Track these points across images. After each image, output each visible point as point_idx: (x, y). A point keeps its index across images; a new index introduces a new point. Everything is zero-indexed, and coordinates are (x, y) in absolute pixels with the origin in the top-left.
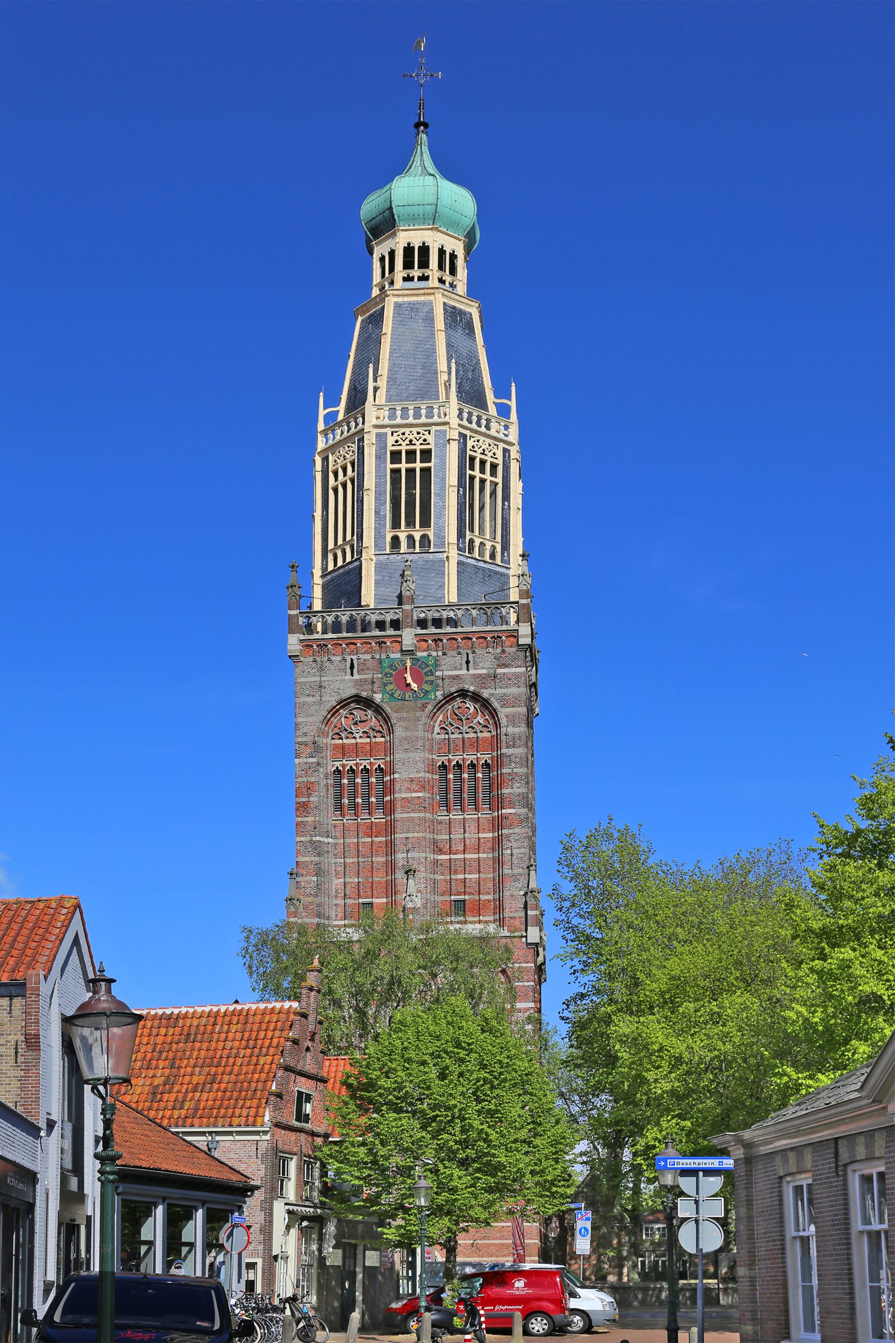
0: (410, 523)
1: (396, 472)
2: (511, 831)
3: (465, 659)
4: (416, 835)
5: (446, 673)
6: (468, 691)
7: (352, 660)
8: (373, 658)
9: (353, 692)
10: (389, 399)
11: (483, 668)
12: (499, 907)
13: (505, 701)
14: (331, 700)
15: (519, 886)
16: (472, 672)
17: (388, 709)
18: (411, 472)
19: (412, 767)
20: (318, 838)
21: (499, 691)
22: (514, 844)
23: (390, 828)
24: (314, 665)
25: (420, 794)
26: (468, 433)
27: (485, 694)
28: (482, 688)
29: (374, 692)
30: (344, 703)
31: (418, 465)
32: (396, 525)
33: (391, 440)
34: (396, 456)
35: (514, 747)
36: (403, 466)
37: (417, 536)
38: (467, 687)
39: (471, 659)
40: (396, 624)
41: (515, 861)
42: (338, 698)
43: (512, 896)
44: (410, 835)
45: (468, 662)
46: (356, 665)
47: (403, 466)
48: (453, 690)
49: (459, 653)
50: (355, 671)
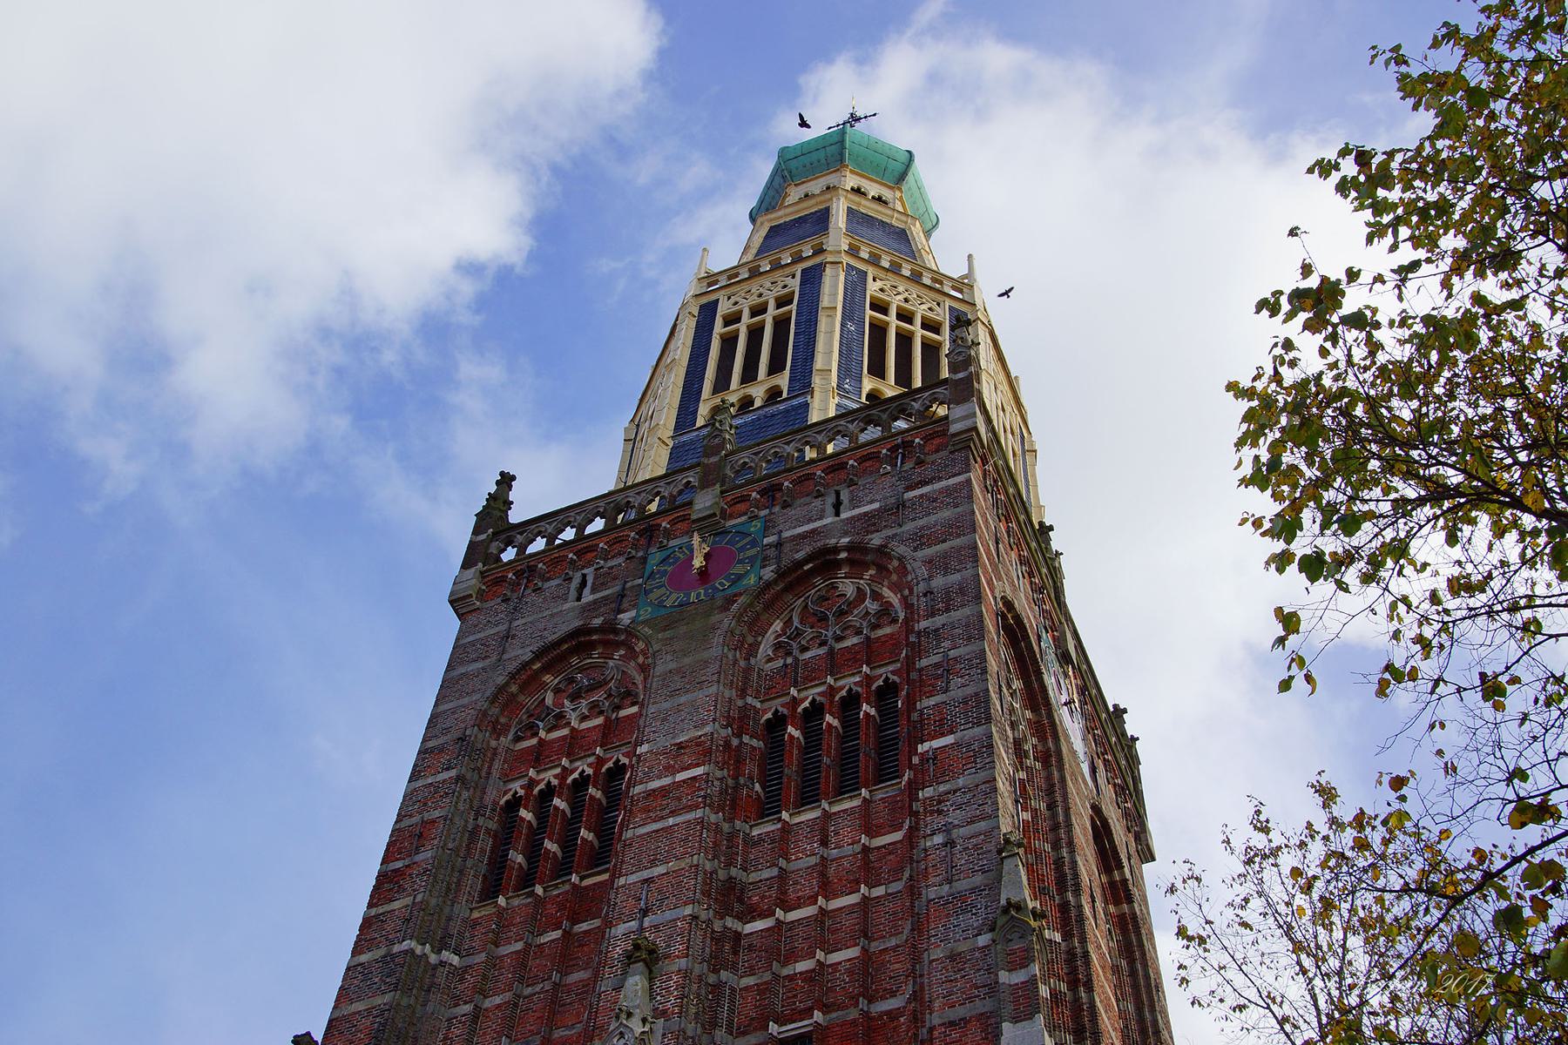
0: (749, 375)
1: (729, 342)
2: (942, 788)
3: (831, 499)
5: (786, 534)
6: (836, 550)
7: (584, 576)
9: (577, 623)
11: (872, 502)
13: (920, 540)
14: (521, 652)
15: (975, 922)
16: (844, 516)
18: (755, 334)
20: (406, 945)
21: (909, 527)
22: (955, 817)
25: (699, 771)
26: (871, 272)
28: (868, 532)
29: (620, 612)
30: (555, 655)
35: (947, 610)
41: (961, 860)
43: (953, 957)
46: (589, 584)
48: (800, 555)
49: (819, 495)
50: (587, 591)
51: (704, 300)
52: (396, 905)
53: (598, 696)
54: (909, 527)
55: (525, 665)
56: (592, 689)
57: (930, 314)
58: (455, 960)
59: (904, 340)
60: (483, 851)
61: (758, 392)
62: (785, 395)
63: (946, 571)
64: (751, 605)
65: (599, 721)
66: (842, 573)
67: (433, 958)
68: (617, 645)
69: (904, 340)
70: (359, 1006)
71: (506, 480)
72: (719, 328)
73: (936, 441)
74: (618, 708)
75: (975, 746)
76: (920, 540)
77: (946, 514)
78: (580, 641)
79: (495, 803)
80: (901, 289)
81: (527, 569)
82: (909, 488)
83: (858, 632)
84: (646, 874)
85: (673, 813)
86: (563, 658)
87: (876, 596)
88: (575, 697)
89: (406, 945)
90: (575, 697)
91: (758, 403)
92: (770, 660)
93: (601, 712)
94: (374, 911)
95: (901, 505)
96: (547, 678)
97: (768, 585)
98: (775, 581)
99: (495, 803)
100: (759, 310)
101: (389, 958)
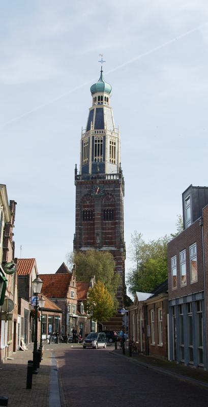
1: (96, 145)
10: (95, 129)
12: (115, 243)
14: (83, 195)
18: (99, 145)
19: (98, 211)
21: (116, 194)
23: (94, 224)
30: (85, 195)
31: (100, 143)
32: (96, 156)
33: (95, 138)
36: (97, 143)
37: (100, 159)
40: (95, 178)
47: (97, 143)
71: (76, 165)
78: (88, 194)
95: (114, 190)
100: (99, 142)
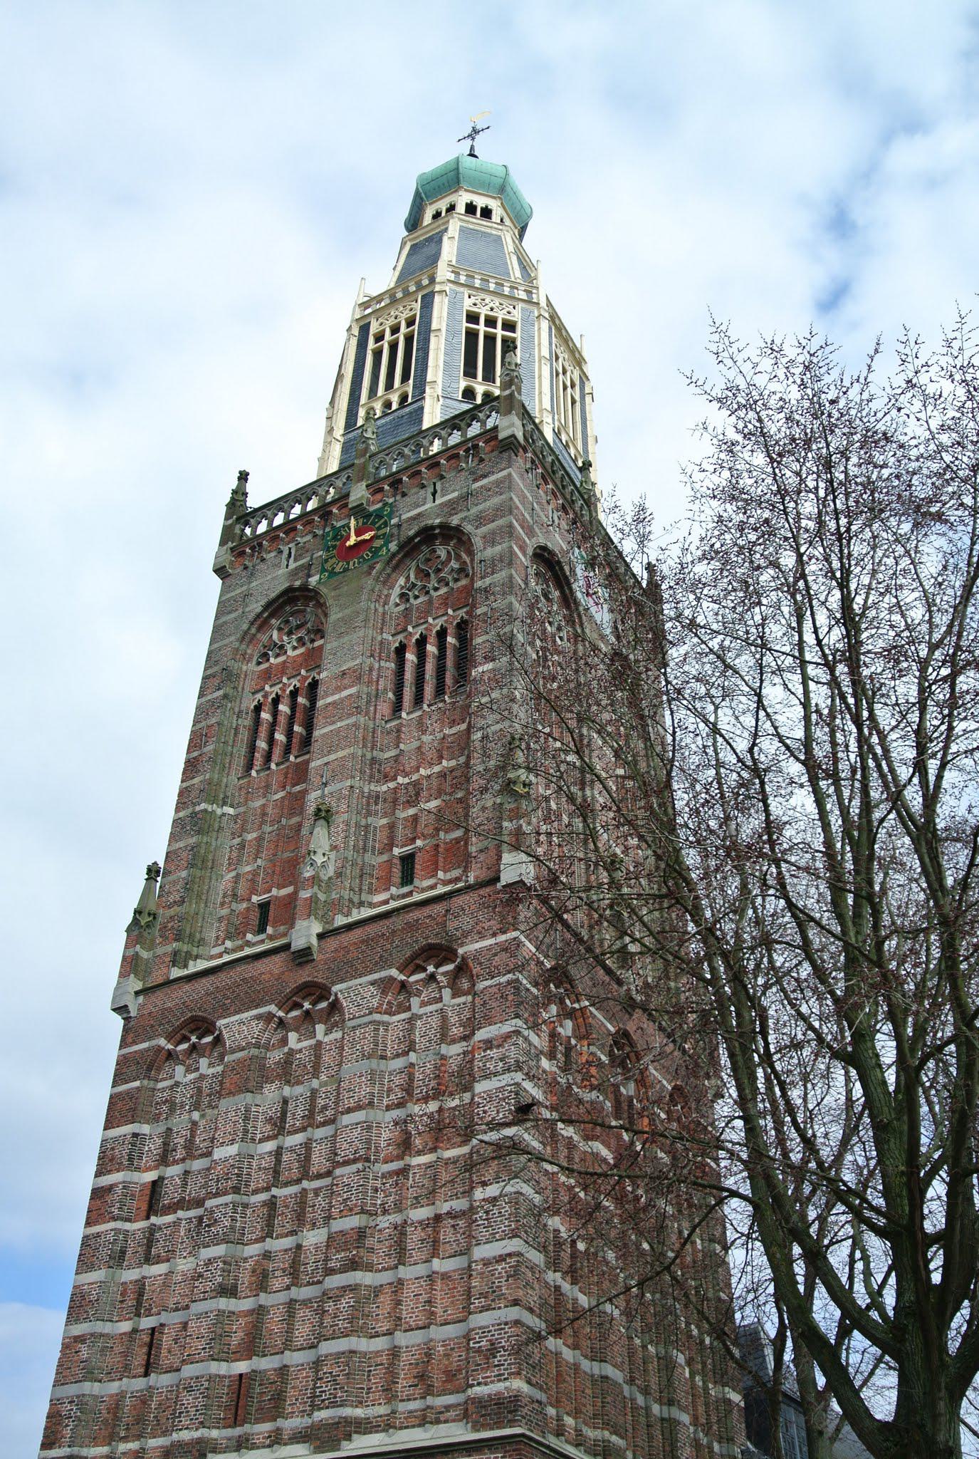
0: (389, 386)
1: (378, 354)
3: (431, 489)
4: (340, 754)
5: (404, 517)
6: (432, 528)
8: (315, 536)
13: (480, 520)
14: (256, 607)
16: (438, 502)
17: (324, 590)
18: (394, 347)
20: (203, 806)
24: (244, 573)
27: (455, 521)
28: (451, 515)
29: (309, 576)
34: (379, 337)
35: (493, 573)
38: (430, 522)
39: (438, 487)
42: (263, 603)
44: (332, 757)
45: (434, 494)
48: (411, 533)
51: (362, 323)
52: (196, 781)
53: (302, 633)
54: (474, 510)
55: (259, 616)
56: (299, 627)
57: (508, 317)
58: (231, 811)
59: (490, 339)
60: (242, 741)
61: (395, 399)
62: (410, 400)
63: (493, 544)
64: (384, 569)
65: (301, 650)
66: (437, 542)
67: (219, 811)
68: (311, 599)
69: (490, 339)
70: (181, 844)
71: (243, 477)
72: (371, 344)
73: (492, 443)
74: (312, 641)
75: (503, 671)
76: (480, 520)
77: (496, 500)
79: (248, 708)
80: (487, 301)
81: (257, 544)
82: (475, 480)
83: (447, 584)
84: (326, 760)
85: (340, 719)
86: (281, 607)
87: (458, 557)
88: (290, 633)
89: (203, 806)
90: (290, 633)
91: (395, 406)
92: (397, 605)
93: (304, 644)
94: (185, 785)
96: (273, 621)
97: (394, 555)
98: (398, 552)
99: (248, 708)
100: (395, 330)
101: (194, 815)
